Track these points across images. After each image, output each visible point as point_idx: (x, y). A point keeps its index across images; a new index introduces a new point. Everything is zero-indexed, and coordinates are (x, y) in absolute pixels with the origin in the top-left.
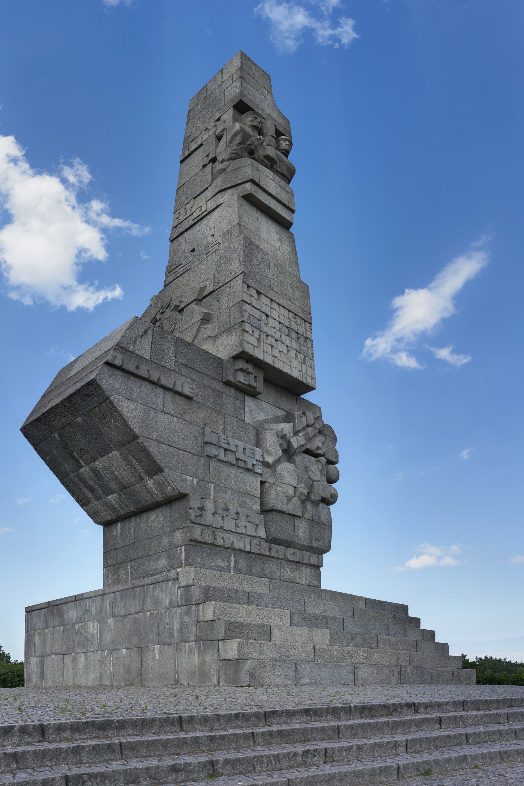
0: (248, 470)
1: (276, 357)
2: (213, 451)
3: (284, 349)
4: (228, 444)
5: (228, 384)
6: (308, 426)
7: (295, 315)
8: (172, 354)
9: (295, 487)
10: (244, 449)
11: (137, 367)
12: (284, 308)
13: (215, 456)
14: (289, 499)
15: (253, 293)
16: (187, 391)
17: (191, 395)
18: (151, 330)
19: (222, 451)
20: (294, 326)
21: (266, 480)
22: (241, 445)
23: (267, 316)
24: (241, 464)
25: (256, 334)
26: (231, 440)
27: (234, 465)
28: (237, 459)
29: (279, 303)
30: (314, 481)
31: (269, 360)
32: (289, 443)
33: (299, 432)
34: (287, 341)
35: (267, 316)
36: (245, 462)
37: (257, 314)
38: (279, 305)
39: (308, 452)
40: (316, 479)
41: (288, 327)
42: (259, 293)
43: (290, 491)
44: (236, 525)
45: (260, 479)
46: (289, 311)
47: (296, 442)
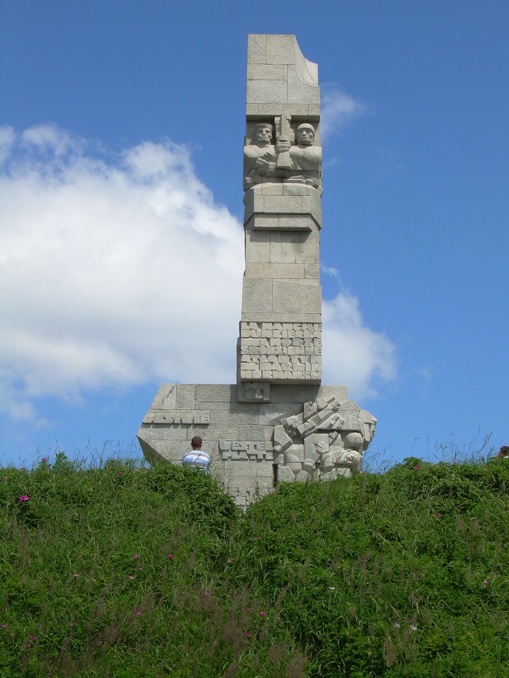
0: (260, 460)
1: (276, 370)
2: (226, 455)
3: (286, 359)
4: (240, 446)
5: (240, 403)
6: (319, 410)
7: (301, 323)
8: (192, 398)
9: (302, 463)
10: (255, 446)
11: (165, 419)
12: (288, 323)
13: (230, 458)
14: (296, 472)
15: (254, 326)
16: (203, 421)
17: (206, 422)
18: (175, 388)
19: (236, 453)
20: (299, 334)
21: (277, 463)
22: (251, 444)
23: (268, 339)
24: (252, 457)
25: (255, 360)
26: (242, 443)
27: (247, 460)
28: (249, 455)
29: (281, 321)
30: (323, 453)
31: (268, 375)
32: (296, 430)
33: (308, 418)
34: (291, 351)
35: (268, 339)
36: (256, 455)
37: (256, 342)
38: (282, 323)
39: (321, 431)
40: (323, 451)
41: (291, 339)
42: (260, 324)
43: (299, 466)
44: (247, 500)
45: (273, 462)
46: (293, 323)
47: (301, 429)
